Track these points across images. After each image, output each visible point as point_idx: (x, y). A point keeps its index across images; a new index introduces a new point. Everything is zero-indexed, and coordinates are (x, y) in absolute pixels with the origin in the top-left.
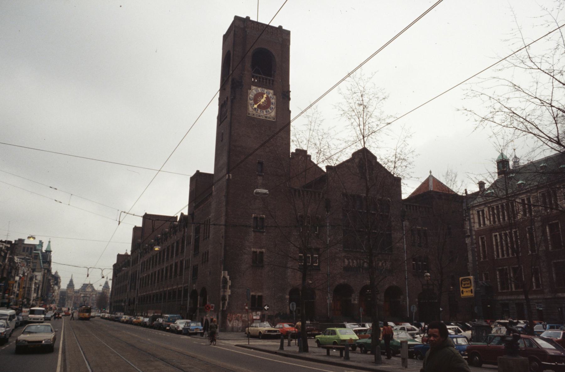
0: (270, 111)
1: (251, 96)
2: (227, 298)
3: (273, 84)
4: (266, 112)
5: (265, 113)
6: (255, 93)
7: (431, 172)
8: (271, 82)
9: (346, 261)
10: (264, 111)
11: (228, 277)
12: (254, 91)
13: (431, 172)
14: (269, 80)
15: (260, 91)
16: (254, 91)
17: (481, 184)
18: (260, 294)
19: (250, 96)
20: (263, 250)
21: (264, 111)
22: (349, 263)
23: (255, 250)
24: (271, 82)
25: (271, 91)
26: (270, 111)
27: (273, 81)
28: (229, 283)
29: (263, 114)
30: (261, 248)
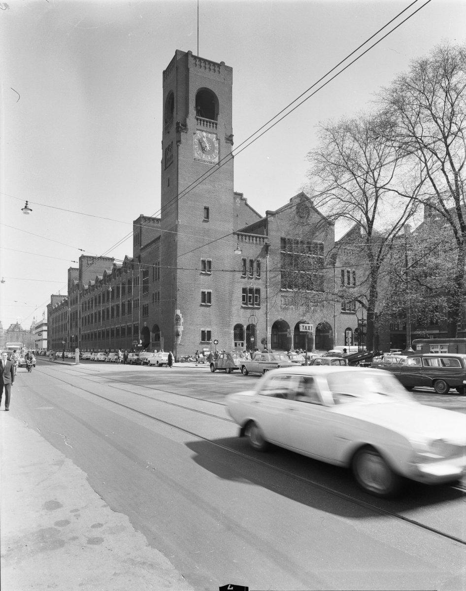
2: (181, 333)
3: (216, 127)
4: (211, 157)
8: (215, 125)
11: (181, 315)
18: (209, 330)
23: (204, 290)
27: (216, 124)
28: (182, 320)
30: (209, 289)
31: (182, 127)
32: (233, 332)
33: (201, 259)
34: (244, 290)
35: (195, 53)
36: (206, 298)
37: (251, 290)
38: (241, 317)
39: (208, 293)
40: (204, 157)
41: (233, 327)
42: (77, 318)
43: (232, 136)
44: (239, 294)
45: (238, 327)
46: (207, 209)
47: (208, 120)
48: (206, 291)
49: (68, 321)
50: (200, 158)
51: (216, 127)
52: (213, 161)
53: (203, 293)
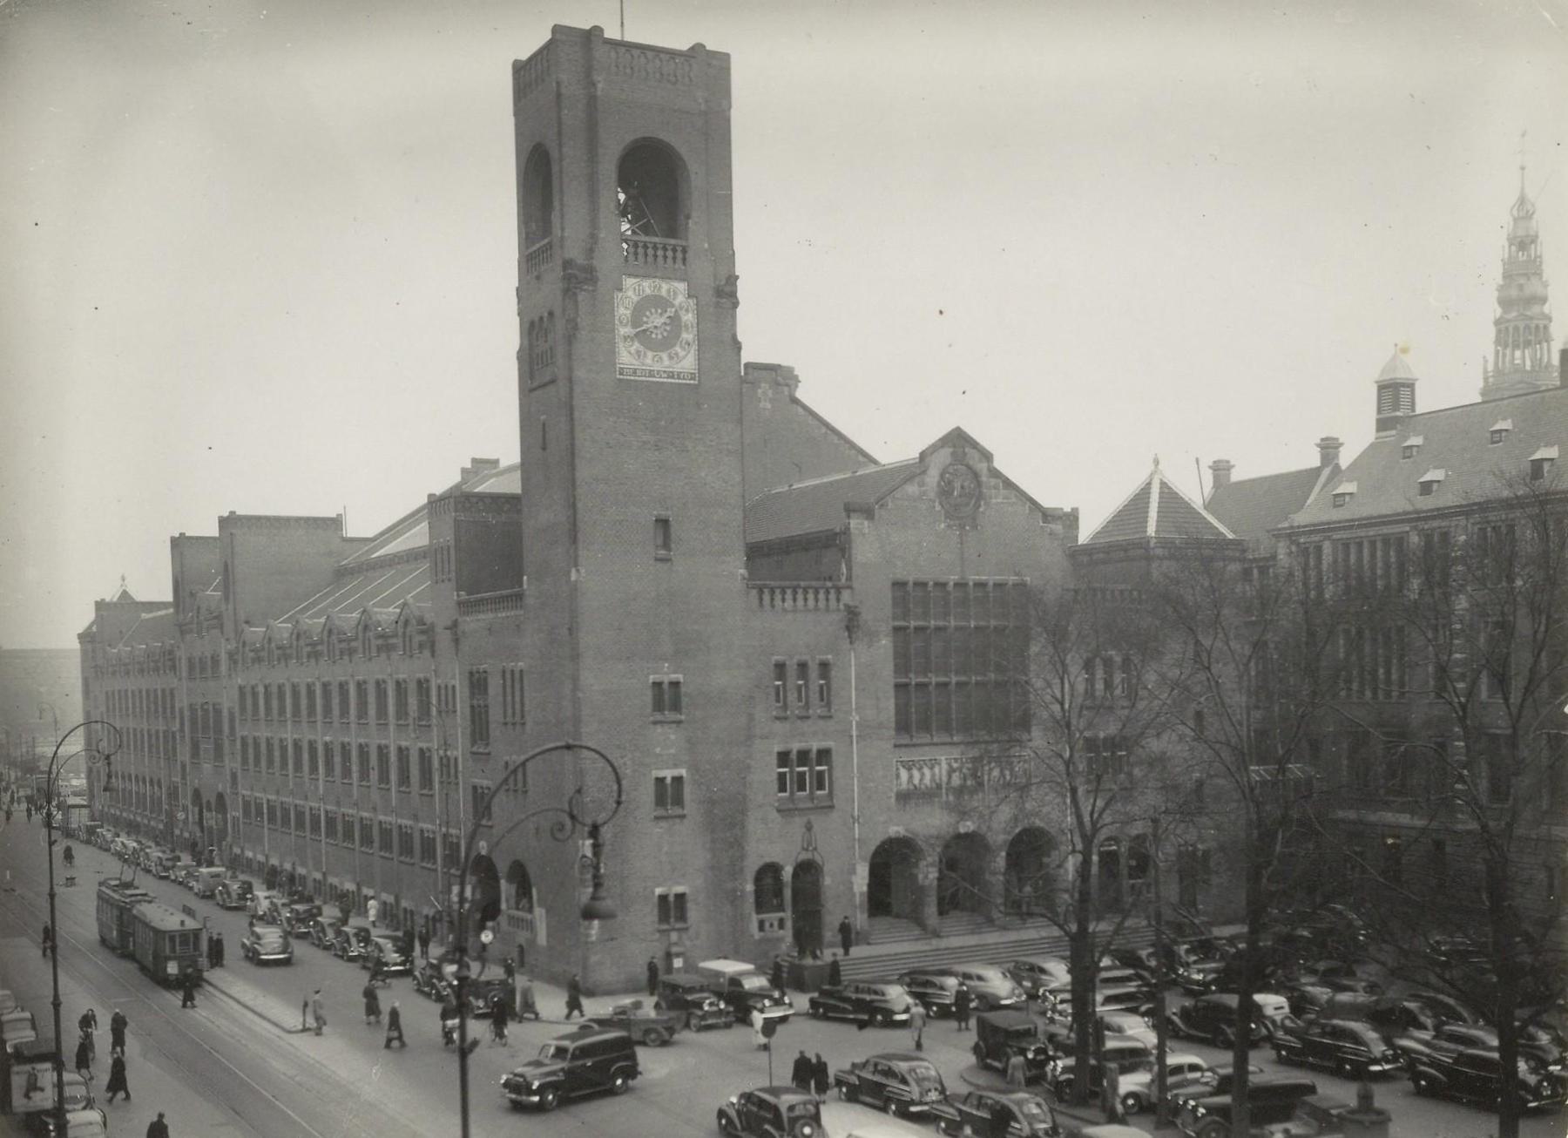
0: (682, 353)
1: (623, 312)
3: (684, 260)
4: (671, 358)
5: (666, 362)
6: (636, 299)
7: (1157, 462)
8: (679, 255)
9: (904, 774)
10: (665, 356)
12: (630, 293)
13: (1157, 462)
14: (674, 250)
15: (648, 291)
16: (630, 293)
17: (1329, 448)
19: (622, 310)
20: (683, 772)
21: (665, 356)
22: (911, 777)
23: (661, 774)
24: (679, 255)
25: (681, 287)
26: (682, 353)
27: (684, 251)
29: (657, 364)
30: (676, 766)
31: (579, 279)
32: (750, 887)
33: (652, 678)
34: (783, 758)
35: (611, 33)
36: (668, 794)
37: (803, 757)
38: (773, 842)
39: (674, 779)
40: (649, 361)
41: (750, 875)
42: (219, 731)
43: (732, 279)
44: (766, 772)
45: (769, 872)
46: (663, 523)
47: (656, 240)
48: (668, 774)
49: (182, 730)
50: (636, 364)
51: (684, 260)
52: (677, 368)
53: (660, 781)
